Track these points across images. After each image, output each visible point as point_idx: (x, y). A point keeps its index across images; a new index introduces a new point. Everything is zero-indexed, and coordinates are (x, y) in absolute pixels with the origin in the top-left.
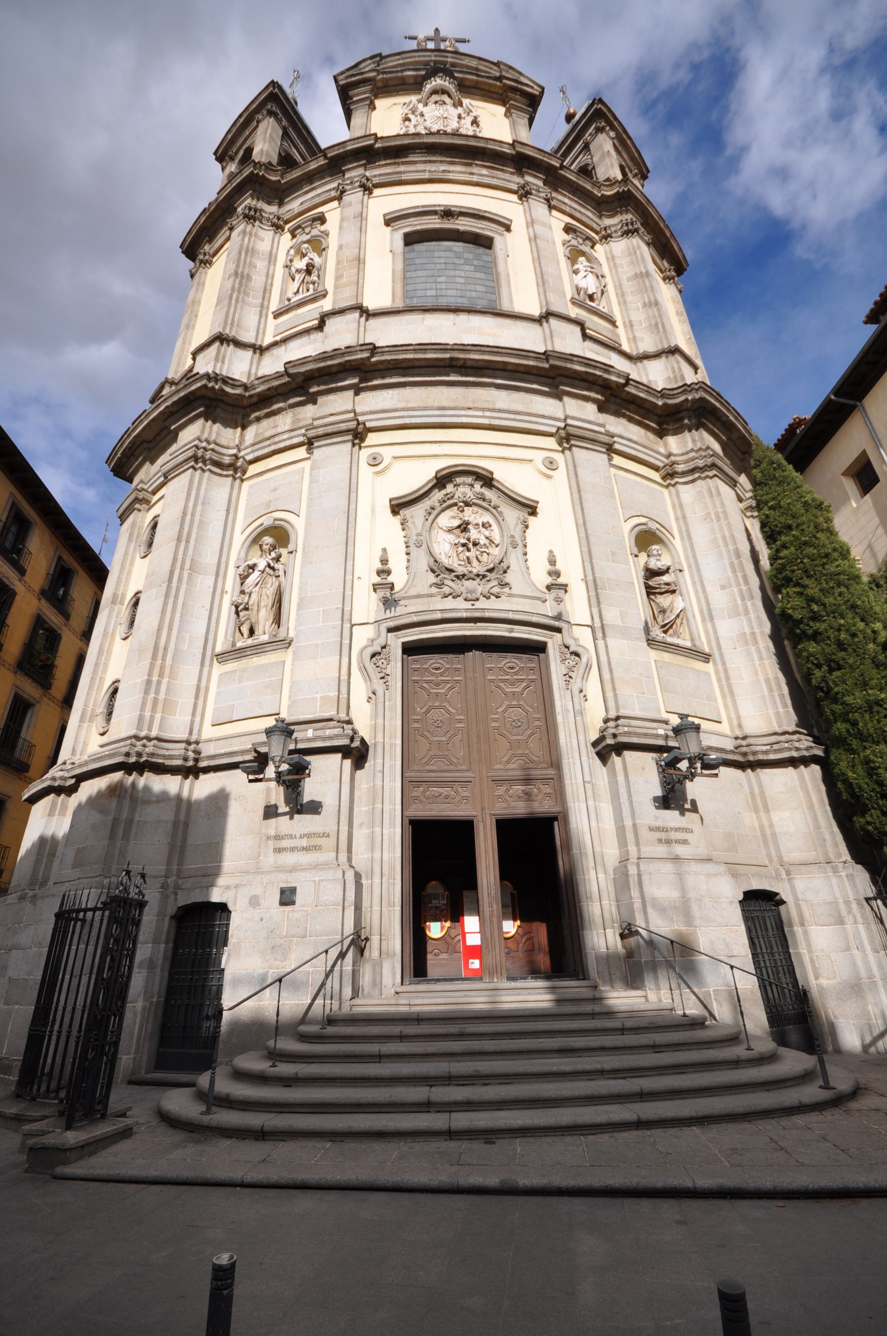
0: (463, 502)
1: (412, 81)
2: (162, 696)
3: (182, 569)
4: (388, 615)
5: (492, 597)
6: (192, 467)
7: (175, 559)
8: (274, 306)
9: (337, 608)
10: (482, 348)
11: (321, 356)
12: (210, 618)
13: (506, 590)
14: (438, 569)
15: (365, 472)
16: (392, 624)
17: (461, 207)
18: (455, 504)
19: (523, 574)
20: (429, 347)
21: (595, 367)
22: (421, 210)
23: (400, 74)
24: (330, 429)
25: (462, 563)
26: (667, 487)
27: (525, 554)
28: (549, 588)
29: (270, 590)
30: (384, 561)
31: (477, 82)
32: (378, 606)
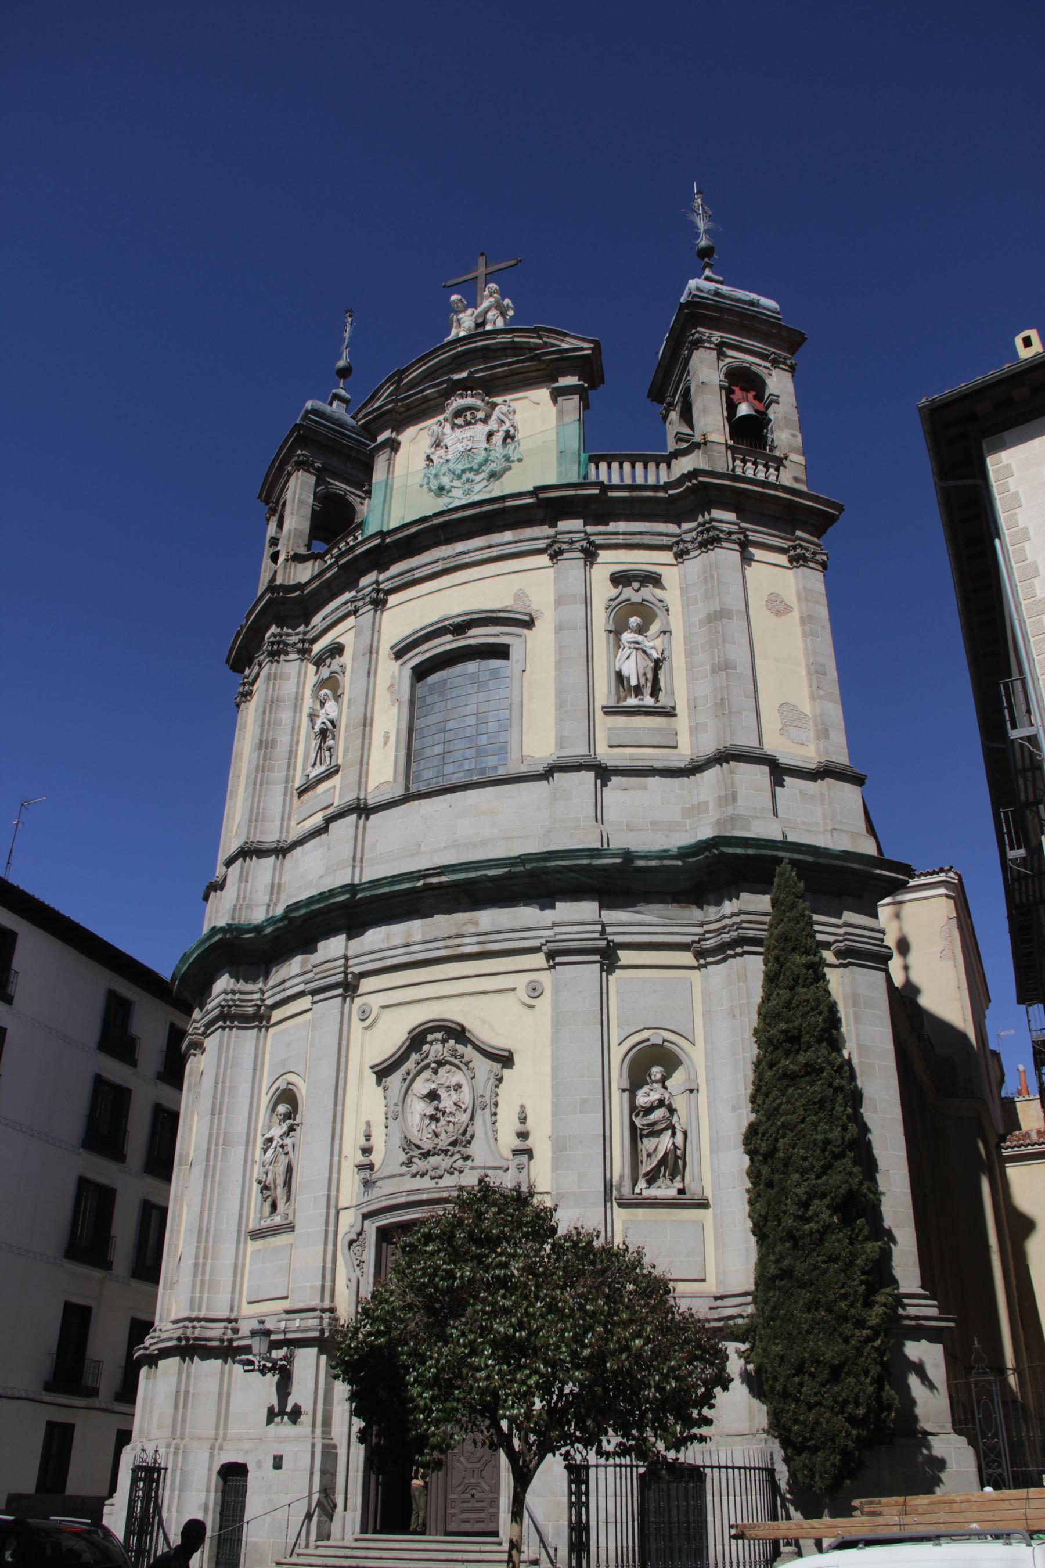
0: (435, 1062)
1: (436, 395)
2: (207, 1277)
3: (217, 1145)
4: (367, 1198)
5: (456, 1172)
6: (220, 1027)
7: (211, 1135)
8: (298, 782)
9: (324, 1195)
12: (243, 1193)
13: (469, 1163)
14: (409, 1145)
15: (356, 1026)
16: (365, 1210)
18: (427, 1066)
19: (488, 1141)
21: (581, 857)
22: (429, 630)
25: (430, 1136)
26: (698, 968)
27: (495, 1114)
28: (516, 1152)
29: (281, 1169)
30: (368, 1137)
32: (359, 1187)
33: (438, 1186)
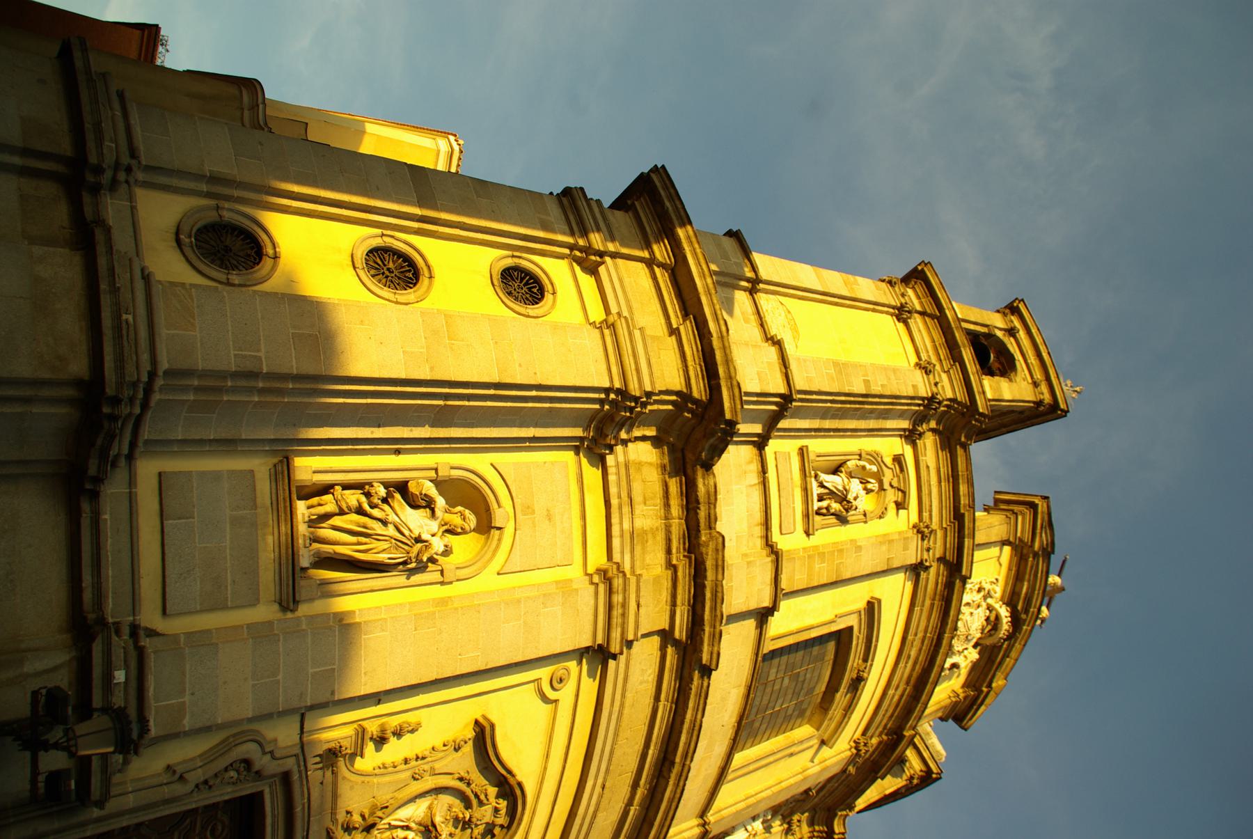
10: (676, 800)
11: (719, 595)
16: (296, 777)
17: (862, 690)
20: (694, 738)
23: (1027, 577)
24: (617, 612)
31: (993, 662)
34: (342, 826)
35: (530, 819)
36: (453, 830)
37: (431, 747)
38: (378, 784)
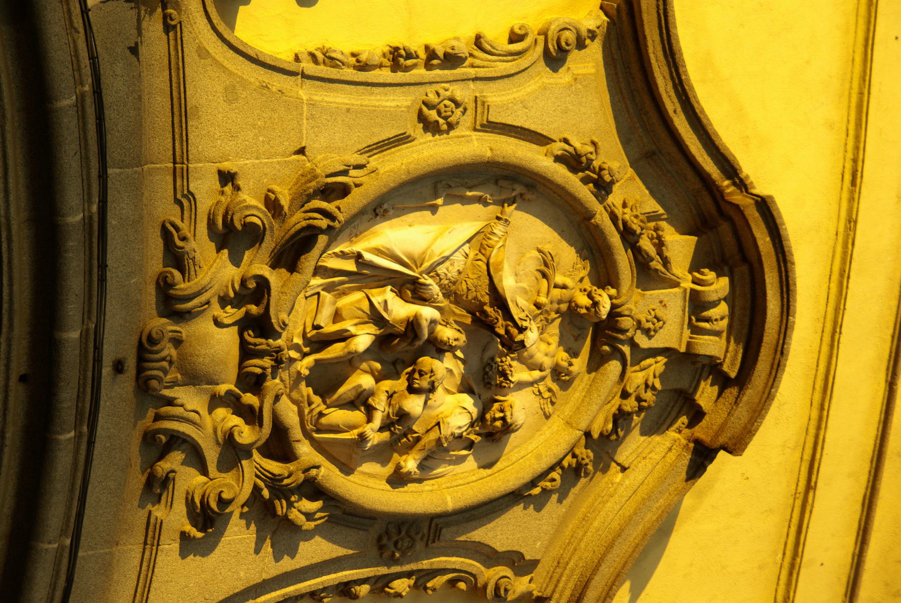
33: (107, 371)
34: (211, 223)
35: (815, 414)
36: (562, 356)
37: (473, 35)
38: (312, 105)
